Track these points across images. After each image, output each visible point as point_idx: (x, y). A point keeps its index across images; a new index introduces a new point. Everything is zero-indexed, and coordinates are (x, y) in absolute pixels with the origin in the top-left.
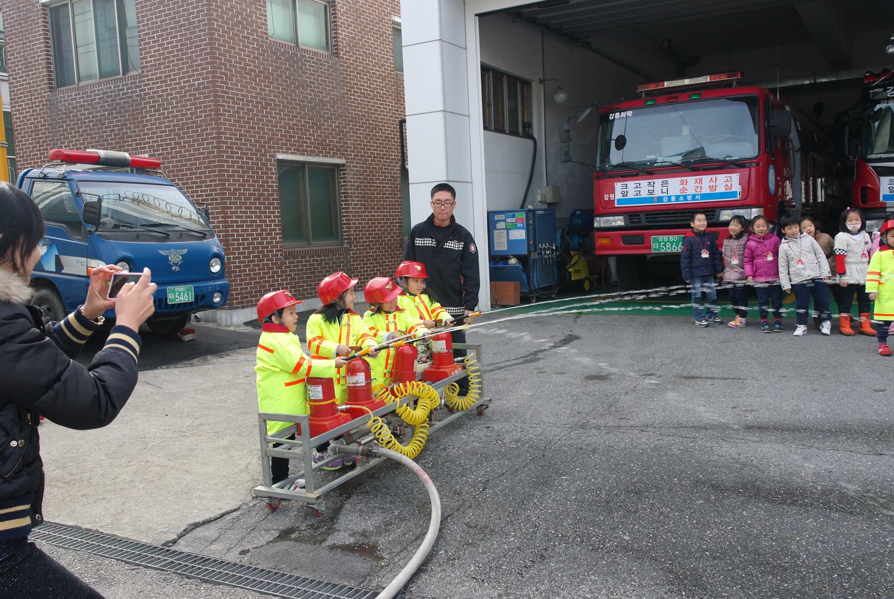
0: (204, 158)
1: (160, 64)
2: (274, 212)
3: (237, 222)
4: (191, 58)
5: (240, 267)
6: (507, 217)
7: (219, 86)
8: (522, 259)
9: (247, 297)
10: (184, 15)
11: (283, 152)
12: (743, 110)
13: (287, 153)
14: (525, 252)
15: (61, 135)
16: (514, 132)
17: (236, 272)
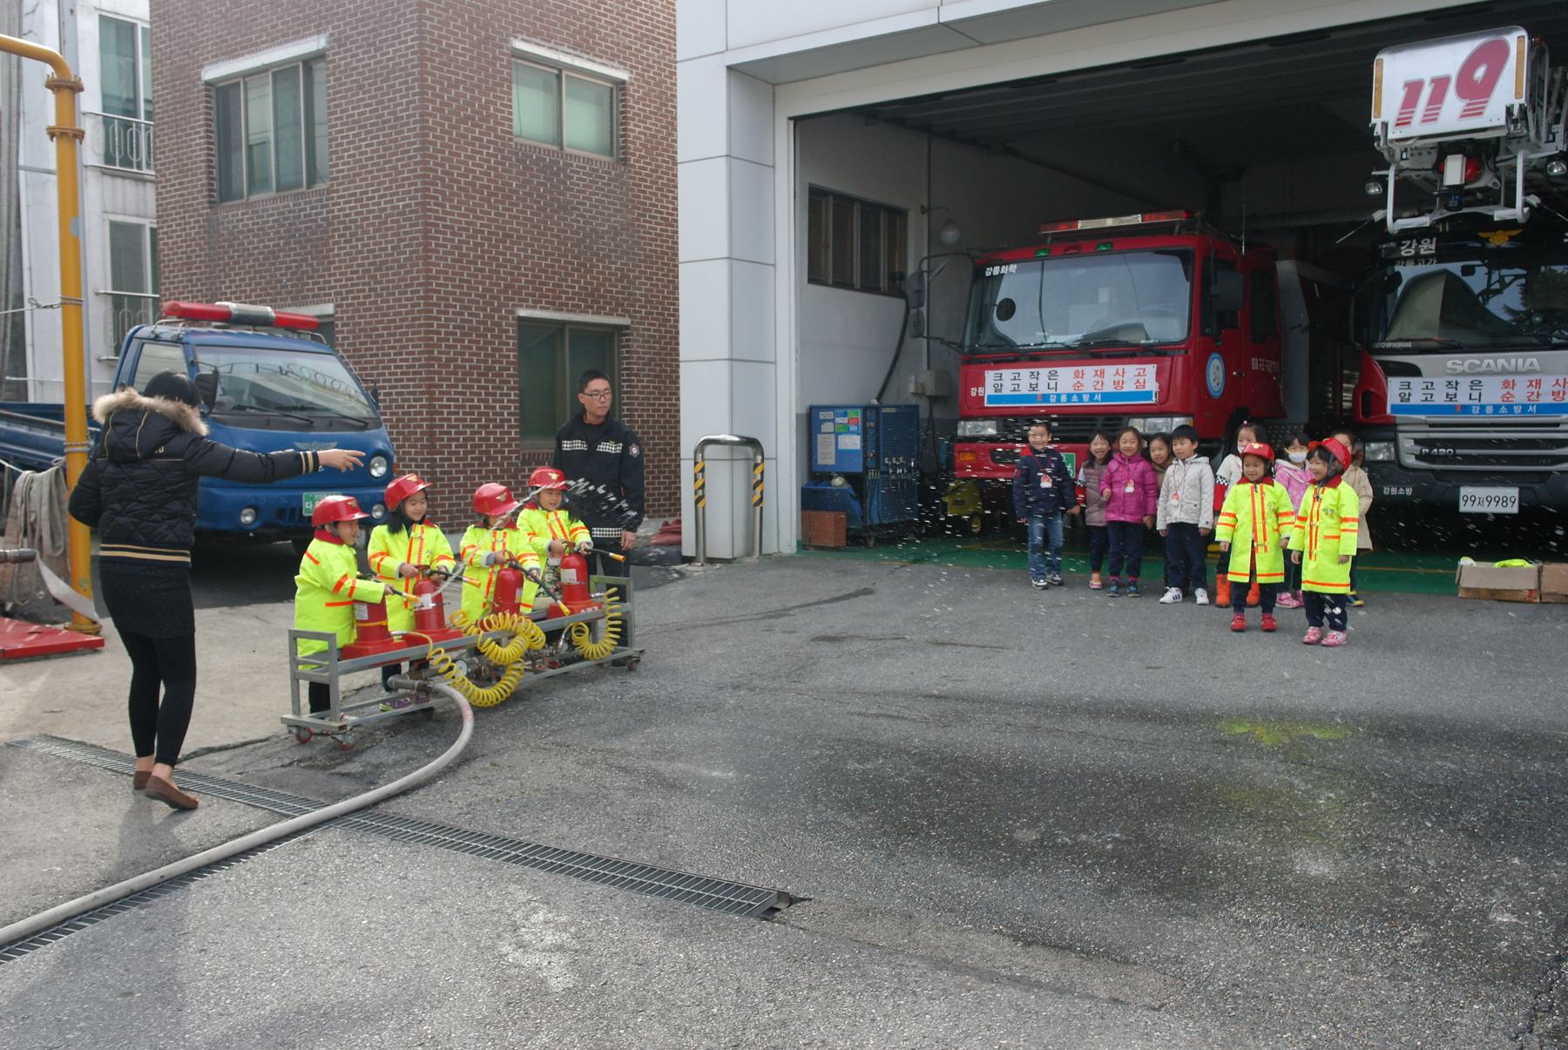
0: (407, 313)
1: (355, 175)
2: (509, 395)
3: (449, 407)
4: (395, 168)
5: (450, 472)
6: (836, 415)
7: (431, 210)
8: (854, 479)
9: (459, 518)
10: (389, 107)
11: (527, 307)
12: (1174, 268)
13: (534, 307)
14: (860, 469)
15: (221, 271)
16: (870, 287)
17: (443, 479)
